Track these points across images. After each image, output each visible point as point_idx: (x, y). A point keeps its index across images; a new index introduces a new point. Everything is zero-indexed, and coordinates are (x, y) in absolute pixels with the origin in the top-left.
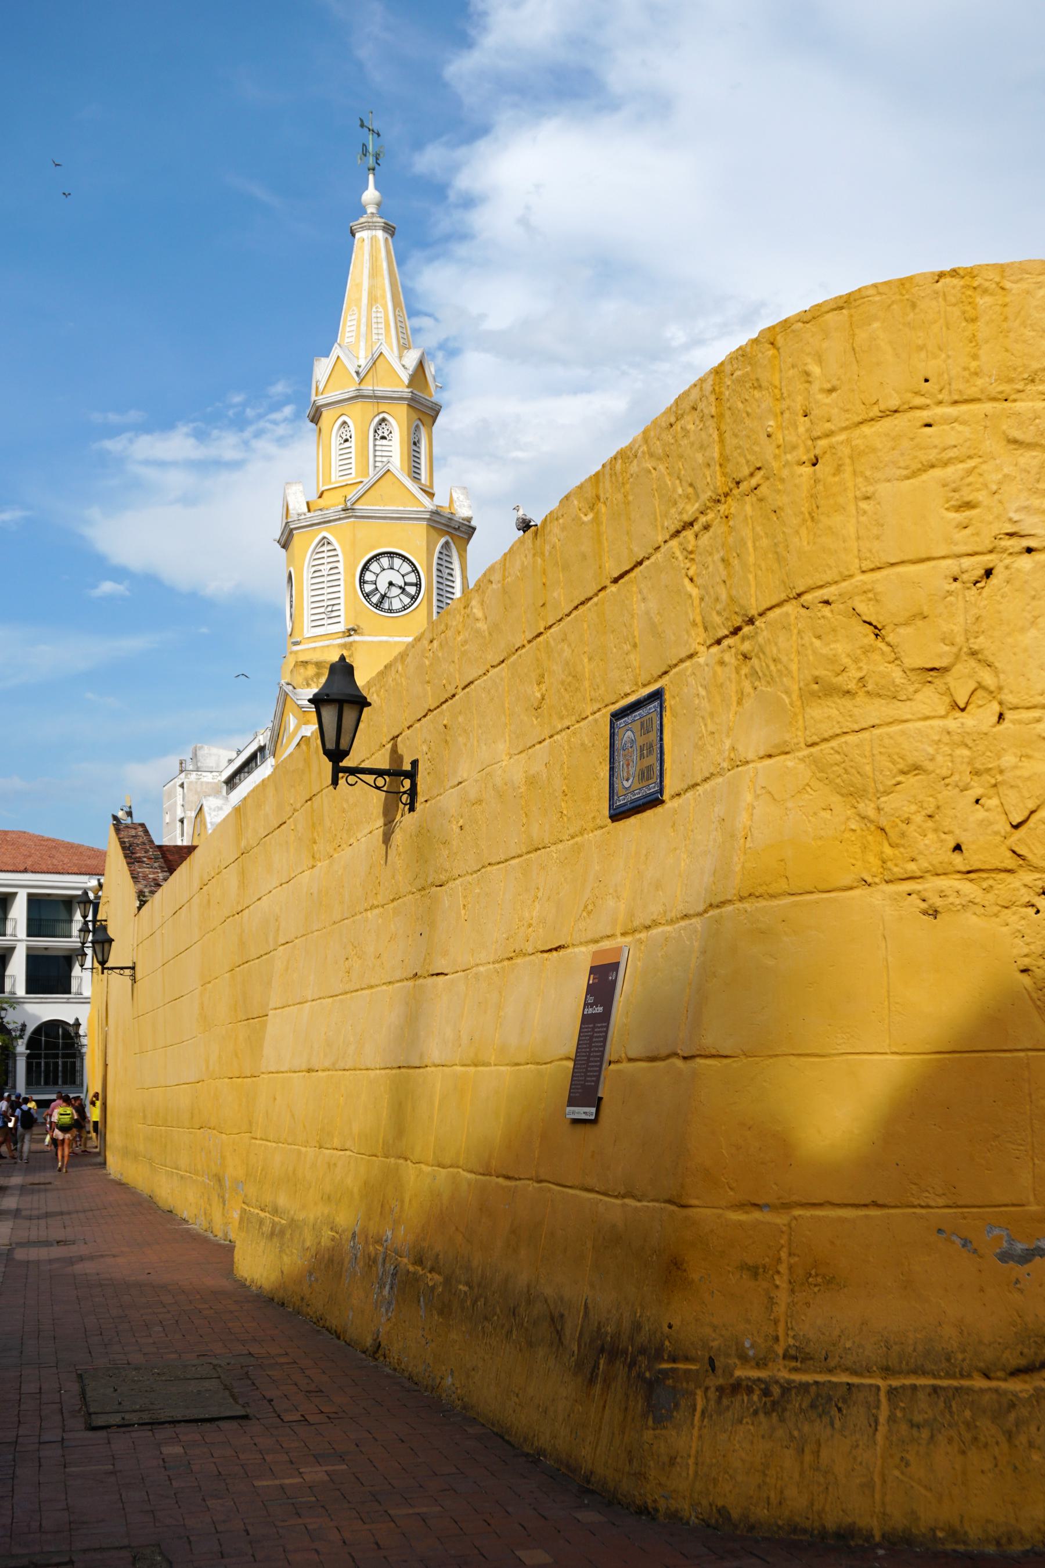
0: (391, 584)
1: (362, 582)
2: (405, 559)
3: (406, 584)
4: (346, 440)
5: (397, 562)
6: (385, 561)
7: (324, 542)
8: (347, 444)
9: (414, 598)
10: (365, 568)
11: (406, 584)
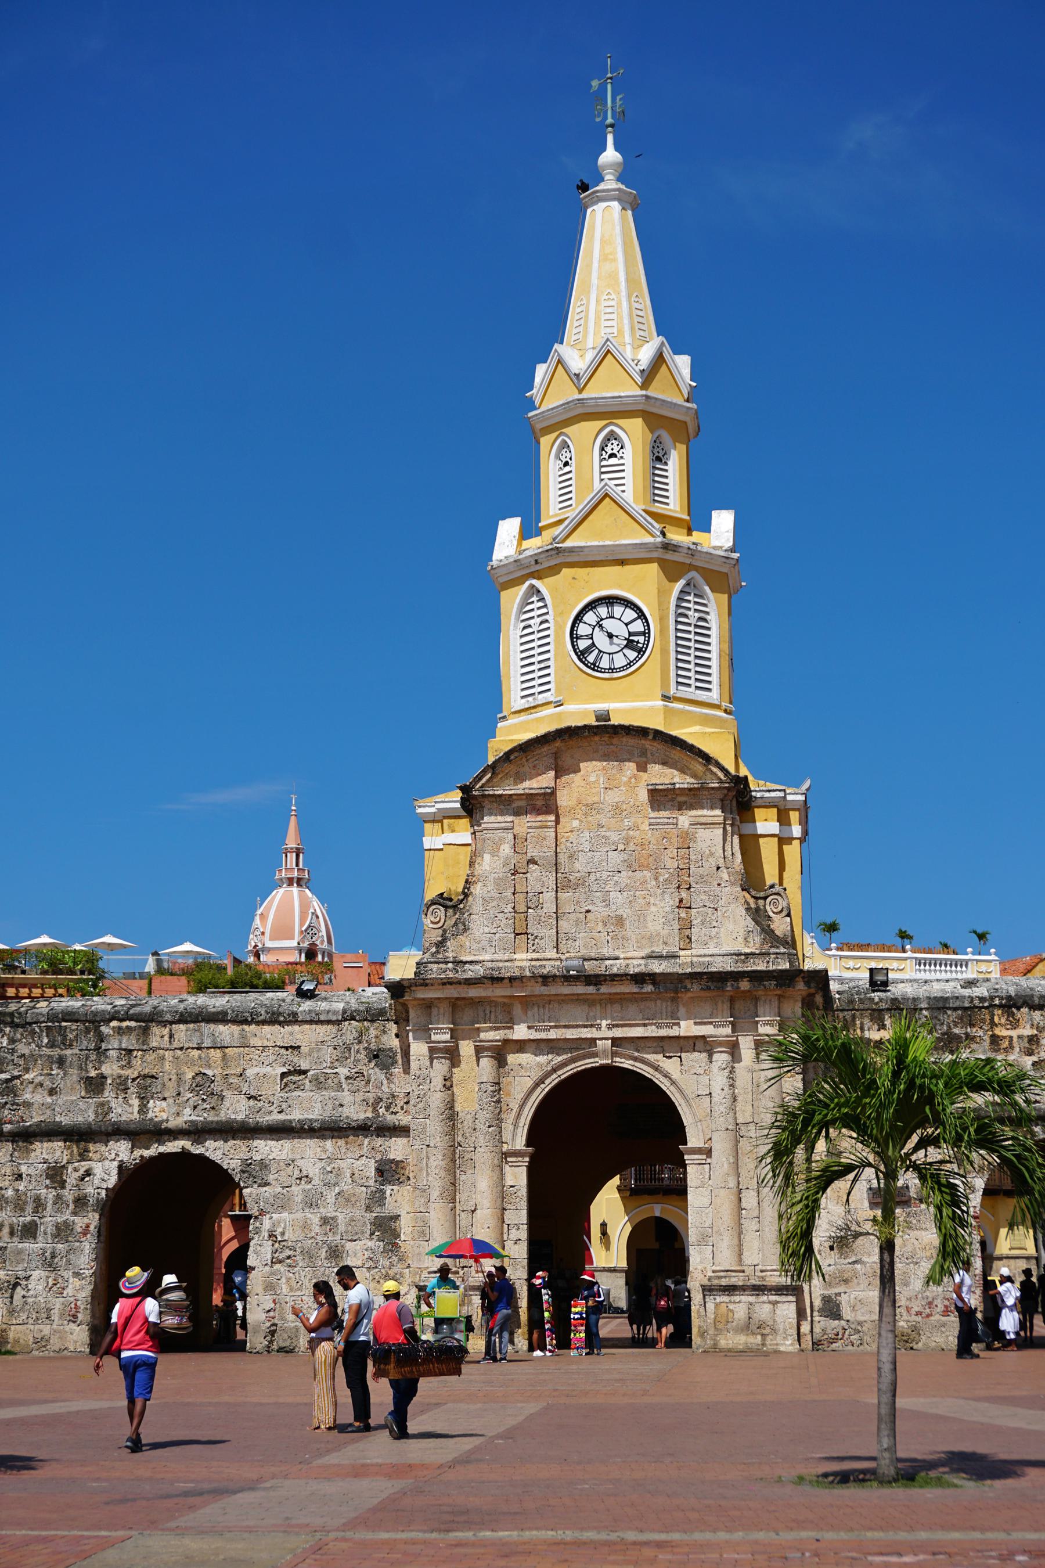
0: (610, 636)
1: (574, 637)
2: (628, 604)
3: (630, 634)
4: (566, 464)
5: (618, 610)
6: (603, 611)
7: (534, 591)
8: (567, 469)
9: (641, 652)
10: (578, 619)
11: (630, 634)
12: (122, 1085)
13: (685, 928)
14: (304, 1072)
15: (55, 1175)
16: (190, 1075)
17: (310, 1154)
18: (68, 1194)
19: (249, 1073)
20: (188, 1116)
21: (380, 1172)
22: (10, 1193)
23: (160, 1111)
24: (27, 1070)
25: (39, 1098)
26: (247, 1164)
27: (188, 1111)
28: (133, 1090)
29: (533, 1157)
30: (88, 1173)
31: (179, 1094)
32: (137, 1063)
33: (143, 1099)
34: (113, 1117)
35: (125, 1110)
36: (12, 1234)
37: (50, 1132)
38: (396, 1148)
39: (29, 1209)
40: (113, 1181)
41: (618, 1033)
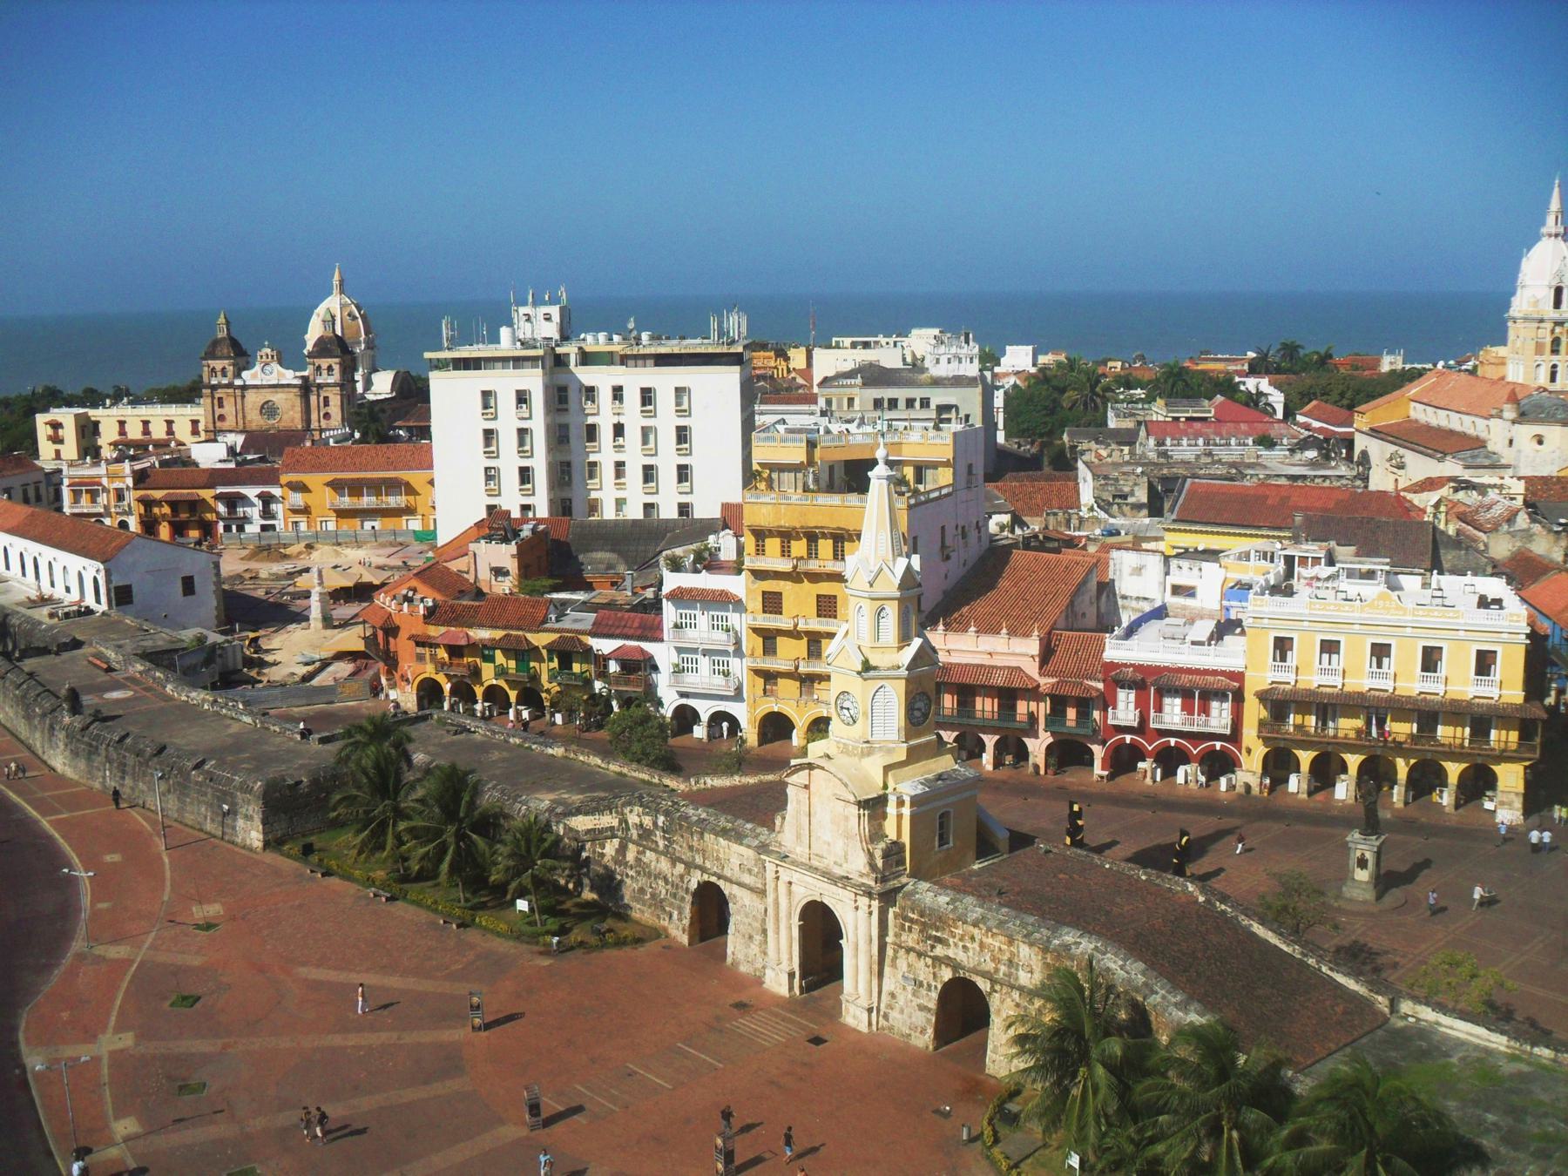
13: (846, 855)
15: (682, 877)
23: (708, 865)
37: (681, 861)
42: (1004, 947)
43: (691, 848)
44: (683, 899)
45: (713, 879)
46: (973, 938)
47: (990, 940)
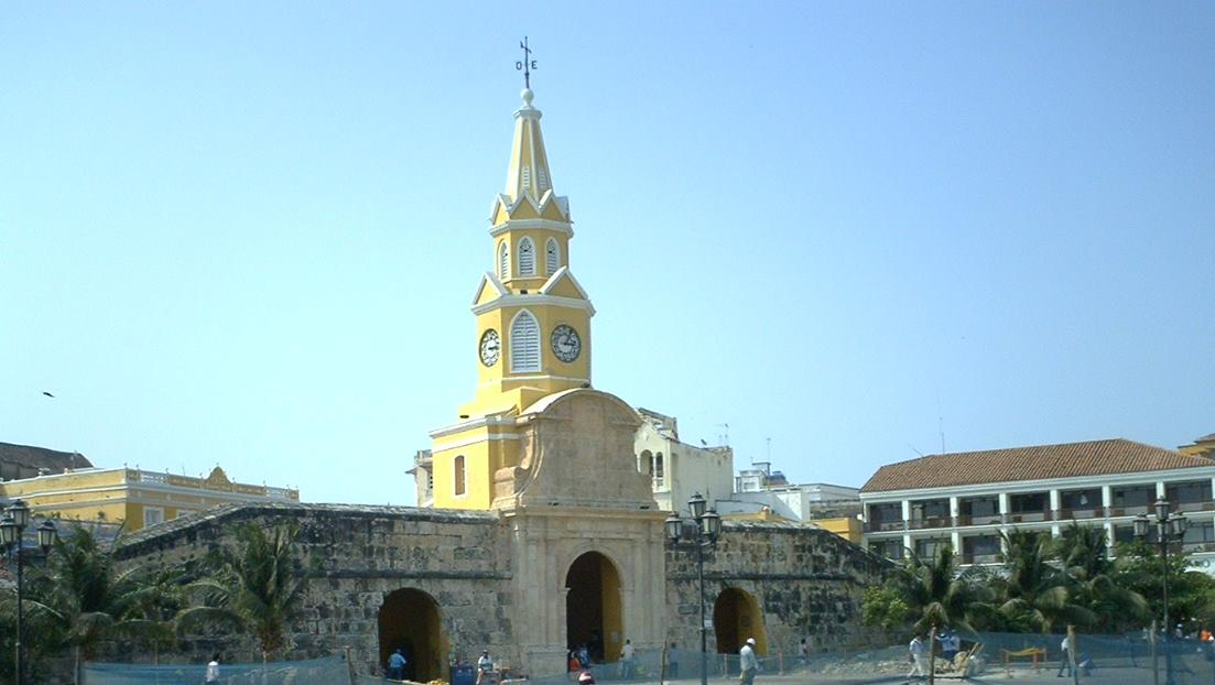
12: (381, 551)
14: (461, 549)
15: (353, 598)
16: (413, 548)
17: (466, 590)
18: (361, 608)
19: (440, 548)
20: (413, 569)
21: (499, 599)
22: (332, 608)
23: (399, 565)
24: (334, 542)
25: (341, 558)
26: (442, 595)
27: (413, 566)
28: (387, 555)
29: (569, 592)
30: (369, 597)
31: (408, 558)
32: (388, 541)
33: (392, 560)
34: (378, 568)
35: (382, 564)
36: (337, 629)
38: (504, 586)
39: (343, 616)
40: (382, 602)
41: (602, 536)
42: (762, 543)
43: (369, 552)
44: (361, 627)
45: (410, 584)
46: (735, 543)
47: (750, 541)
